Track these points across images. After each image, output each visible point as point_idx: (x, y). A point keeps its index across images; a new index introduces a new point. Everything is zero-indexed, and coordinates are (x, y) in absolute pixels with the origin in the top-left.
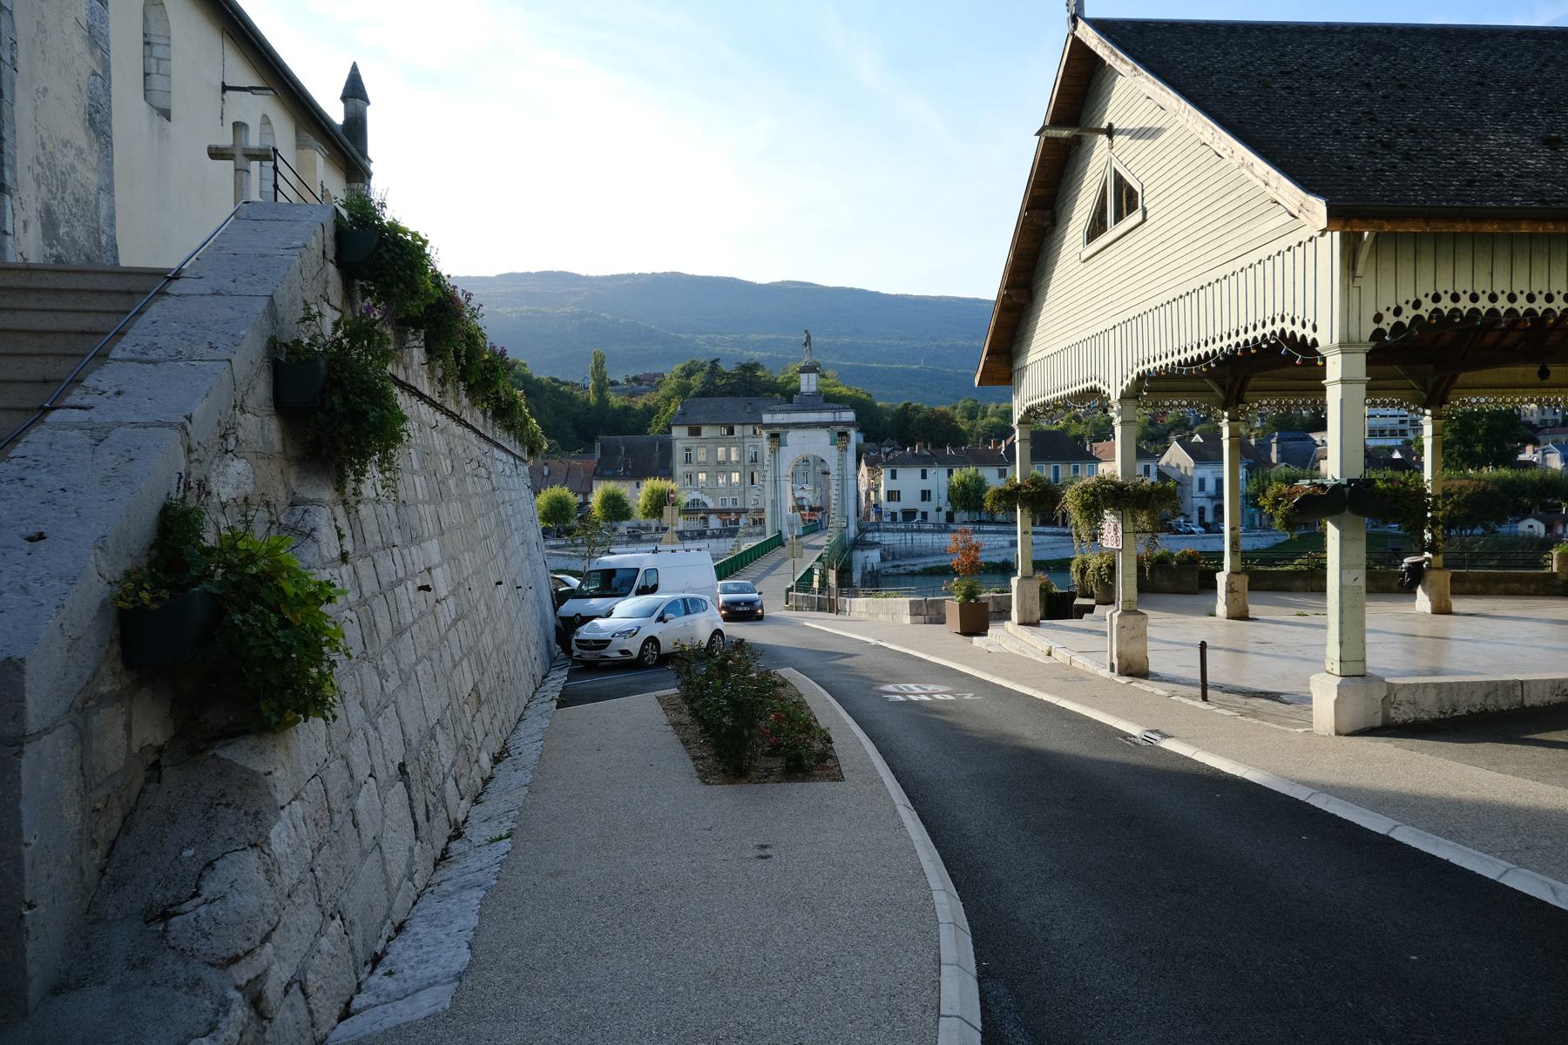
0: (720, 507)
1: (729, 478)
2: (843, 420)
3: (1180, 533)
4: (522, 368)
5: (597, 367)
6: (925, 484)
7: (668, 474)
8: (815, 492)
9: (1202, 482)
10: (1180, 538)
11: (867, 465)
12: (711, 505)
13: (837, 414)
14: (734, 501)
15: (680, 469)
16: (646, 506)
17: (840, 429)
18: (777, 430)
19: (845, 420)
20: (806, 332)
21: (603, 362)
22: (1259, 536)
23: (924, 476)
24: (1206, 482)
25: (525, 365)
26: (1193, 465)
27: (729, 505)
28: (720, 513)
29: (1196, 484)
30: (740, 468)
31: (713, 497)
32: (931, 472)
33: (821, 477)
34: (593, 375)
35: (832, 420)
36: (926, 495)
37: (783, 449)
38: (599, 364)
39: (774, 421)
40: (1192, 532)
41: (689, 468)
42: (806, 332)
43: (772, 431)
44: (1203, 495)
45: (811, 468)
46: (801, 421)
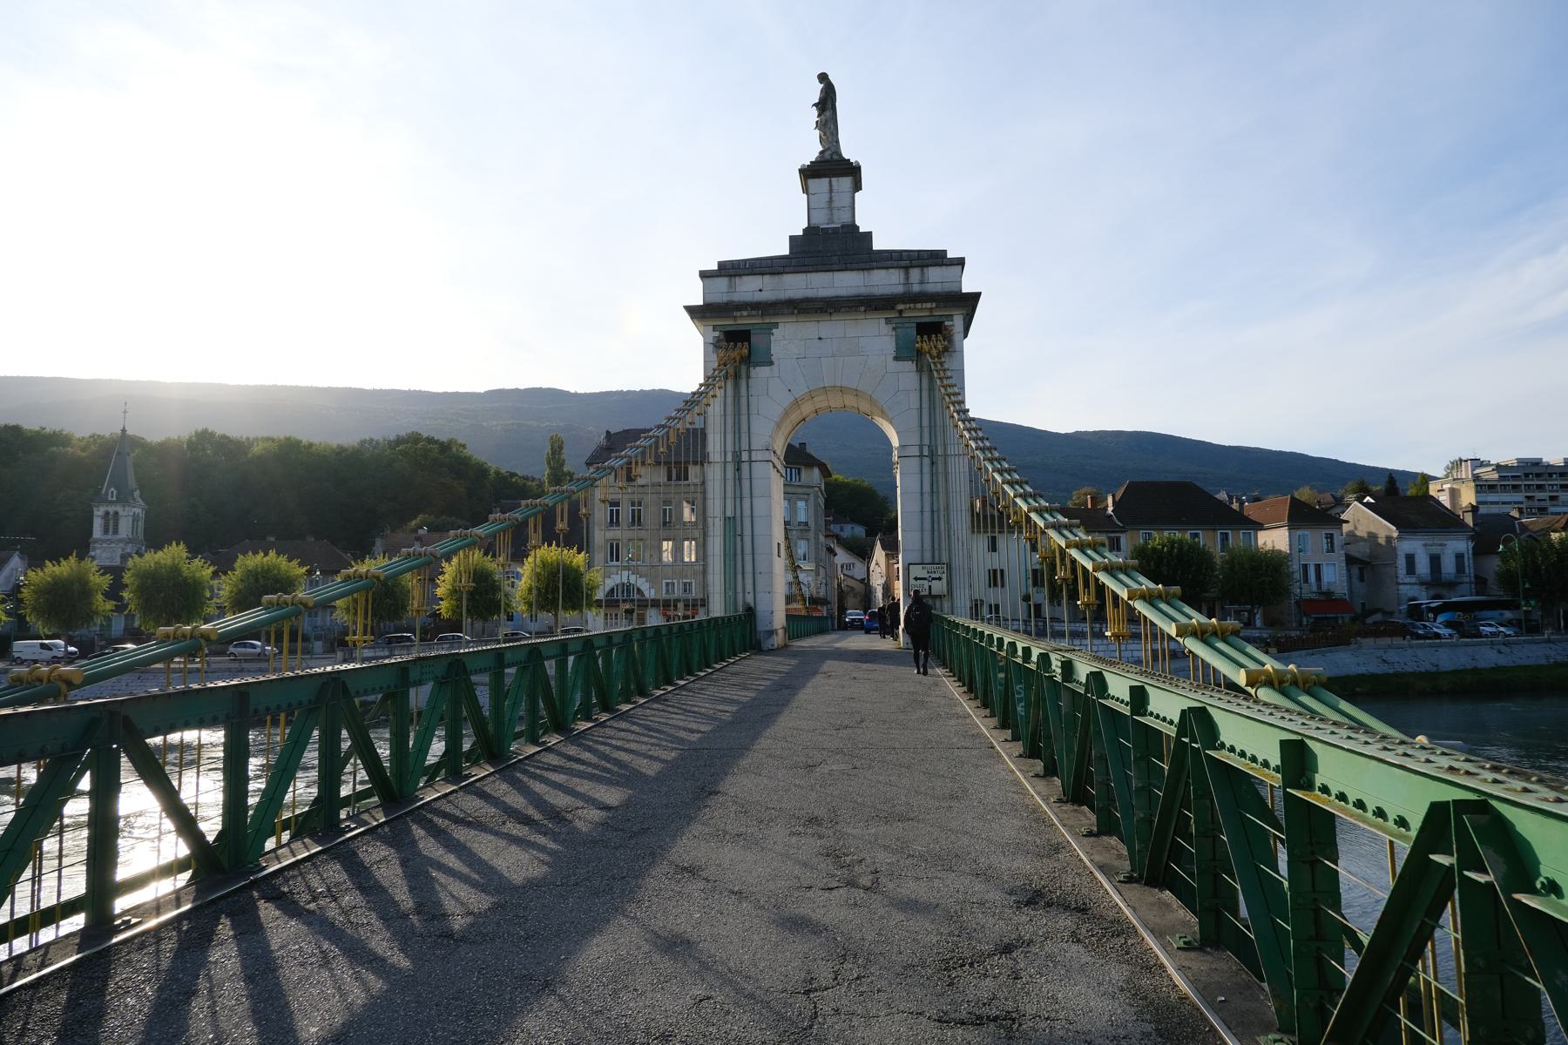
0: (663, 595)
1: (678, 551)
2: (930, 288)
3: (1419, 637)
4: (461, 449)
5: (553, 453)
6: (994, 561)
7: (577, 537)
8: (818, 574)
9: (1410, 559)
10: (1430, 646)
11: (884, 548)
12: (650, 594)
13: (915, 274)
14: (687, 588)
15: (600, 536)
16: (530, 590)
17: (922, 313)
18: (744, 321)
19: (937, 288)
20: (823, 78)
21: (561, 448)
22: (1549, 641)
23: (993, 547)
24: (1417, 559)
25: (464, 446)
26: (1395, 534)
27: (678, 593)
28: (665, 605)
29: (1401, 563)
30: (697, 534)
31: (653, 581)
32: (1002, 542)
33: (823, 553)
34: (549, 463)
35: (900, 289)
36: (996, 578)
37: (759, 373)
38: (557, 448)
39: (737, 297)
40: (1437, 636)
41: (614, 533)
42: (823, 78)
43: (727, 322)
44: (1413, 580)
45: (811, 535)
46: (810, 294)
